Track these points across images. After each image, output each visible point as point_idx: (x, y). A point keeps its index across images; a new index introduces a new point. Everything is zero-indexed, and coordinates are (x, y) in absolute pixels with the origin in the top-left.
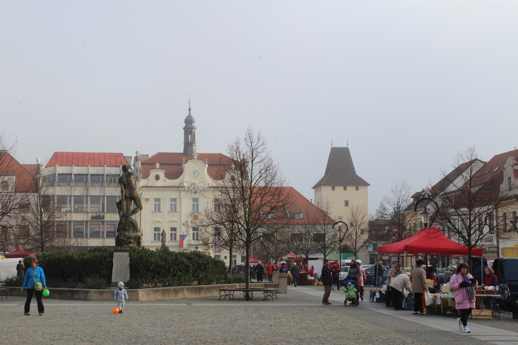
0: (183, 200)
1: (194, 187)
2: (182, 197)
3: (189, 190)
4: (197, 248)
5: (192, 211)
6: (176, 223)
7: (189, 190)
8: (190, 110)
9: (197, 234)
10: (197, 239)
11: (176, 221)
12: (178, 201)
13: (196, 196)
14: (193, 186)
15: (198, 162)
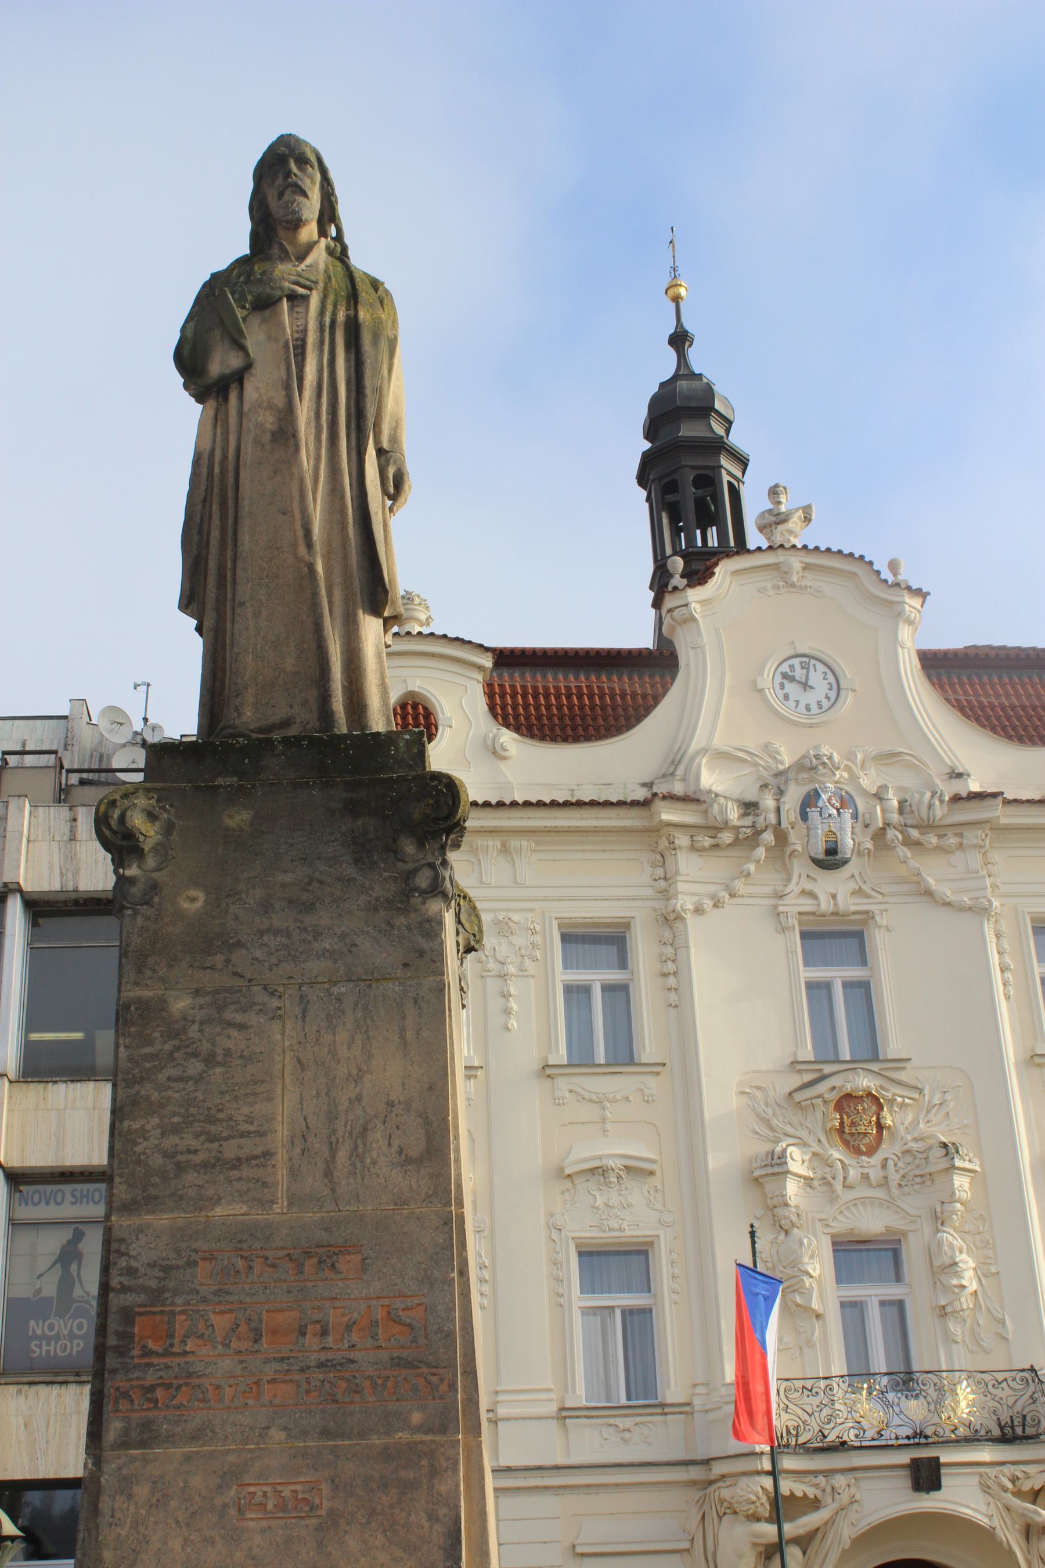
0: (697, 932)
1: (810, 800)
2: (685, 902)
3: (751, 833)
4: (926, 1476)
5: (807, 1052)
6: (636, 1193)
7: (751, 833)
8: (680, 340)
9: (897, 1311)
10: (905, 1380)
11: (636, 1171)
12: (643, 949)
13: (834, 892)
14: (794, 795)
15: (810, 580)
